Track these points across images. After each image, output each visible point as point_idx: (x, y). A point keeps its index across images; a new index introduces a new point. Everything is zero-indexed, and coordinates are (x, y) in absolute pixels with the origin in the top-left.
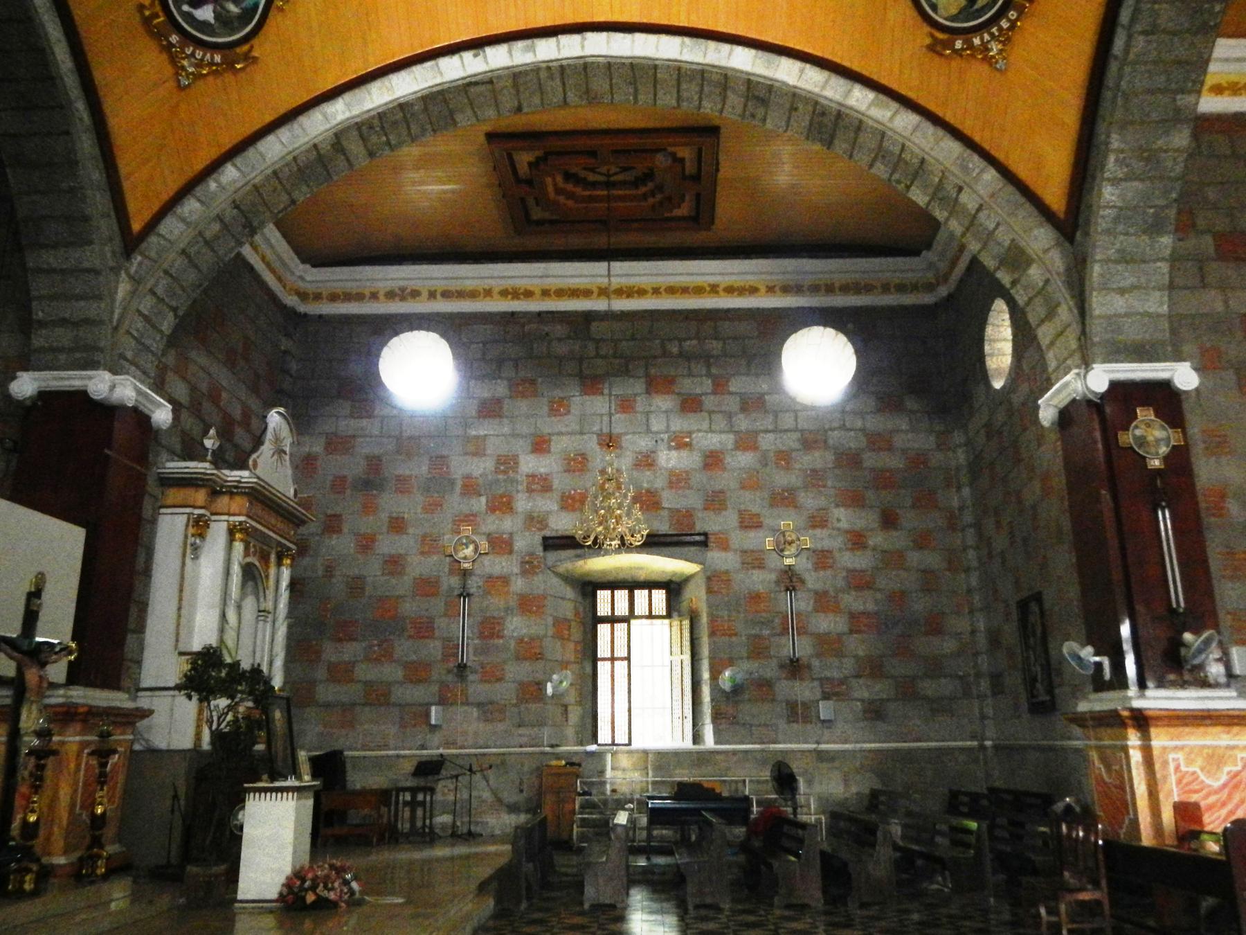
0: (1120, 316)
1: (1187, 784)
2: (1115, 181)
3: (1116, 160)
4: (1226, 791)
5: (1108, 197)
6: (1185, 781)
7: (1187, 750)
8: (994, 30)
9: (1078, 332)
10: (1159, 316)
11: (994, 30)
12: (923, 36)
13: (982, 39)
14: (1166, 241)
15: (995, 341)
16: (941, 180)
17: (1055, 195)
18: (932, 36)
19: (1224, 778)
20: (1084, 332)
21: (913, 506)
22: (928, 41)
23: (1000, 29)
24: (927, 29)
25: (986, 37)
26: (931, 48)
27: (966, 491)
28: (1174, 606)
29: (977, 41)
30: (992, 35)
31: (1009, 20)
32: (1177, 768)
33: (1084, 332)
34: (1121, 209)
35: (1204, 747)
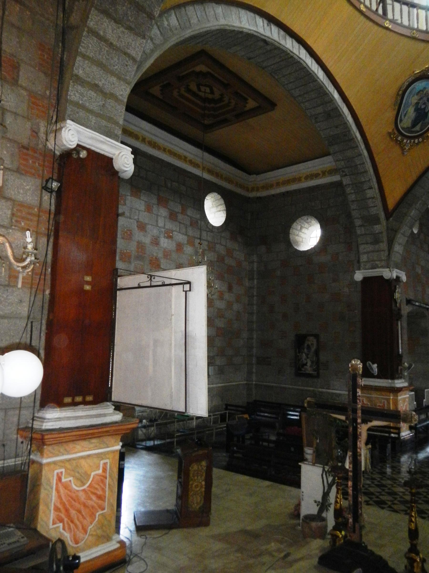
8: (412, 141)
11: (412, 141)
12: (391, 128)
13: (407, 141)
15: (294, 229)
16: (365, 181)
17: (391, 203)
18: (393, 130)
20: (389, 254)
22: (390, 131)
23: (414, 142)
24: (393, 126)
25: (409, 141)
26: (389, 134)
27: (255, 282)
29: (405, 141)
30: (410, 142)
31: (418, 141)
33: (389, 254)
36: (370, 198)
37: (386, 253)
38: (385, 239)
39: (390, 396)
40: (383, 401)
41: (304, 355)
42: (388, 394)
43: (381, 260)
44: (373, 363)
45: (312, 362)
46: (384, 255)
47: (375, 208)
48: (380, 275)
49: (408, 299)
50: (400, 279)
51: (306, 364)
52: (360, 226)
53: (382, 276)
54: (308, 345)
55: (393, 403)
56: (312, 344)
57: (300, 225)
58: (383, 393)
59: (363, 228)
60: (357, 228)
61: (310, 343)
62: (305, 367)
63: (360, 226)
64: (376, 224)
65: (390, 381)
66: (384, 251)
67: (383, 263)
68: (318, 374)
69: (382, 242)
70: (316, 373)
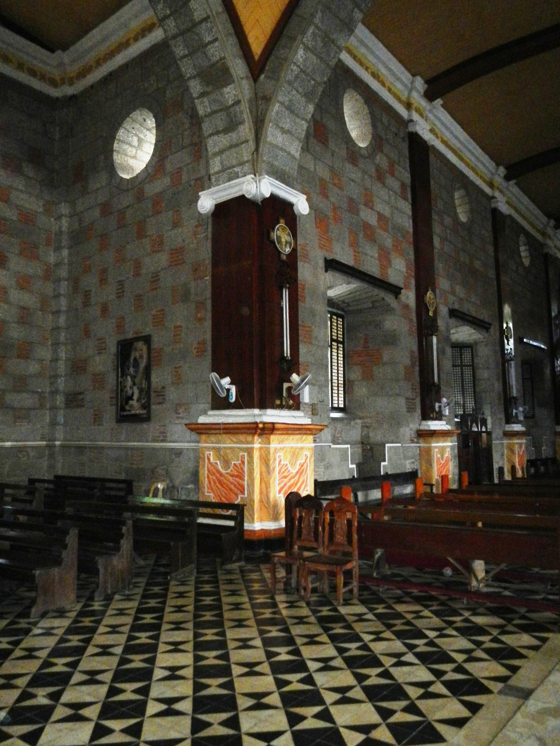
0: (277, 147)
1: (283, 473)
2: (306, 48)
3: (313, 33)
4: (297, 477)
5: (299, 57)
6: (282, 471)
7: (285, 450)
9: (253, 149)
10: (293, 157)
14: (311, 108)
15: (123, 142)
19: (298, 467)
20: (257, 149)
21: (21, 253)
27: (65, 252)
28: (285, 355)
32: (280, 461)
33: (257, 149)
34: (302, 71)
35: (292, 447)
36: (201, 22)
37: (252, 144)
38: (247, 116)
39: (252, 442)
40: (241, 454)
41: (129, 378)
42: (249, 438)
43: (242, 164)
44: (222, 377)
45: (141, 390)
46: (246, 152)
47: (217, 44)
48: (240, 194)
49: (328, 259)
50: (295, 208)
51: (131, 398)
52: (203, 95)
53: (243, 196)
54: (135, 359)
55: (261, 457)
56: (141, 357)
57: (136, 135)
58: (242, 437)
59: (205, 99)
60: (196, 101)
61: (137, 355)
62: (131, 402)
63: (203, 95)
64: (226, 85)
65: (256, 411)
66: (247, 141)
67: (247, 167)
68: (149, 412)
69: (242, 123)
70: (144, 412)
